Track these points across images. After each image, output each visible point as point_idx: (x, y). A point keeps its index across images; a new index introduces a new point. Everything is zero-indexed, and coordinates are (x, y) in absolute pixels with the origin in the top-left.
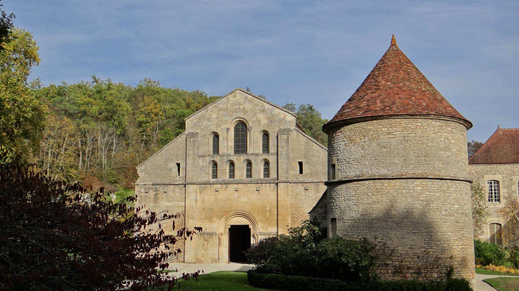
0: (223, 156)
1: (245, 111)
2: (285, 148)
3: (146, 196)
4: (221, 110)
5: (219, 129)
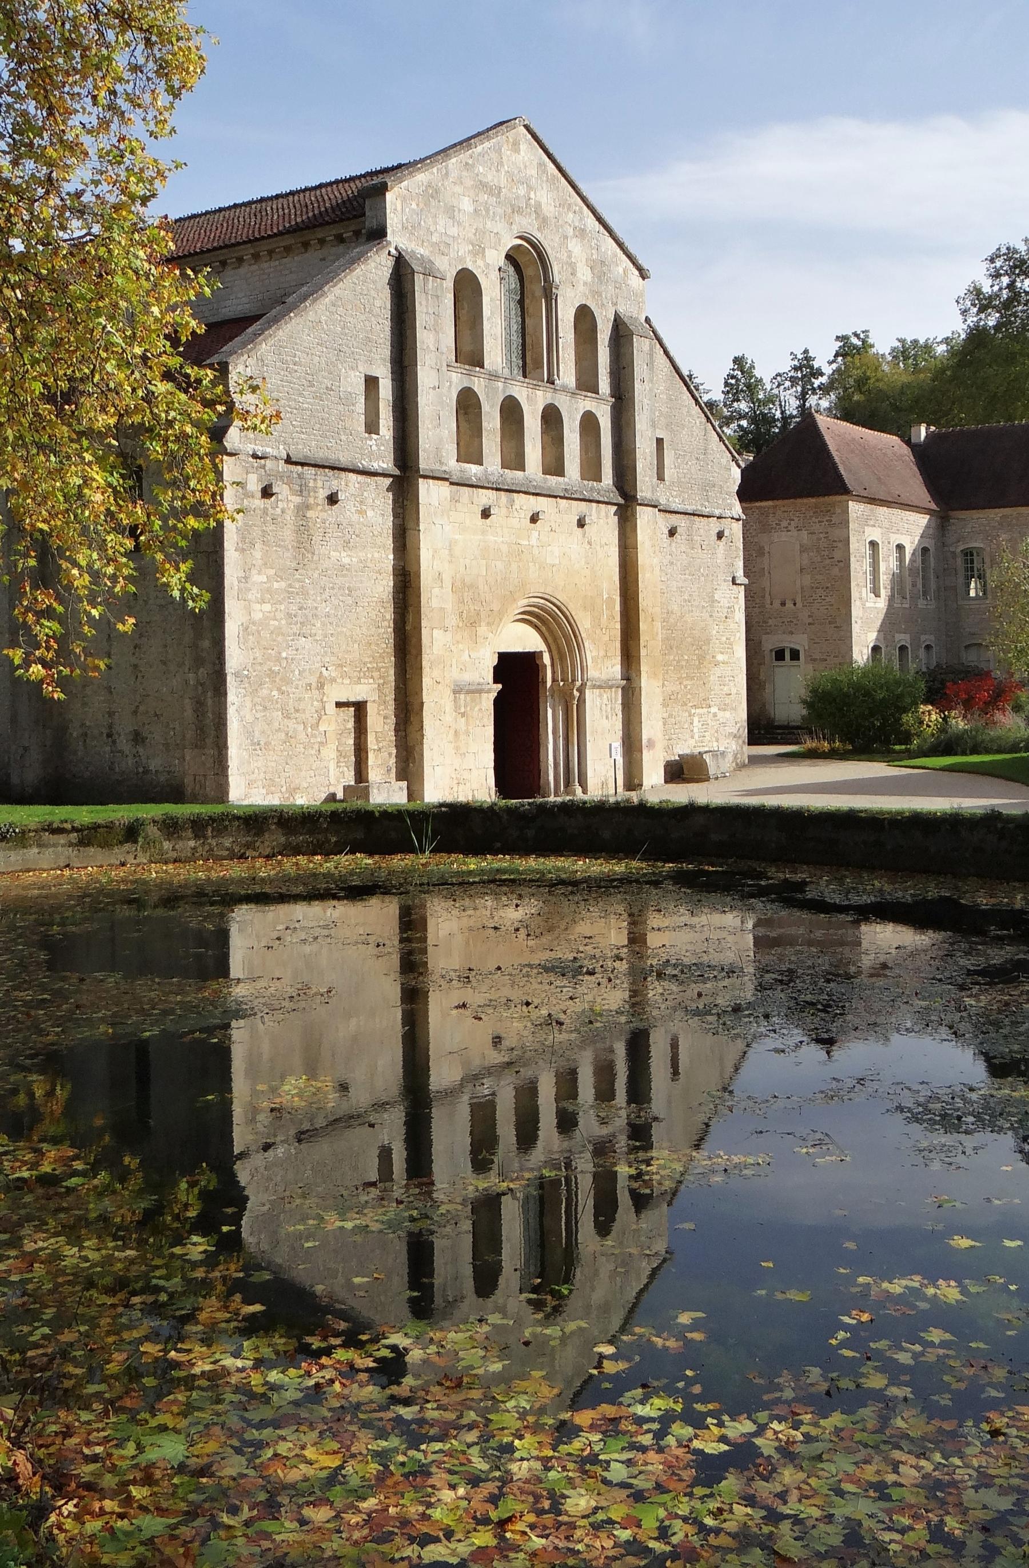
0: (493, 376)
3: (265, 511)
4: (483, 186)
5: (480, 263)
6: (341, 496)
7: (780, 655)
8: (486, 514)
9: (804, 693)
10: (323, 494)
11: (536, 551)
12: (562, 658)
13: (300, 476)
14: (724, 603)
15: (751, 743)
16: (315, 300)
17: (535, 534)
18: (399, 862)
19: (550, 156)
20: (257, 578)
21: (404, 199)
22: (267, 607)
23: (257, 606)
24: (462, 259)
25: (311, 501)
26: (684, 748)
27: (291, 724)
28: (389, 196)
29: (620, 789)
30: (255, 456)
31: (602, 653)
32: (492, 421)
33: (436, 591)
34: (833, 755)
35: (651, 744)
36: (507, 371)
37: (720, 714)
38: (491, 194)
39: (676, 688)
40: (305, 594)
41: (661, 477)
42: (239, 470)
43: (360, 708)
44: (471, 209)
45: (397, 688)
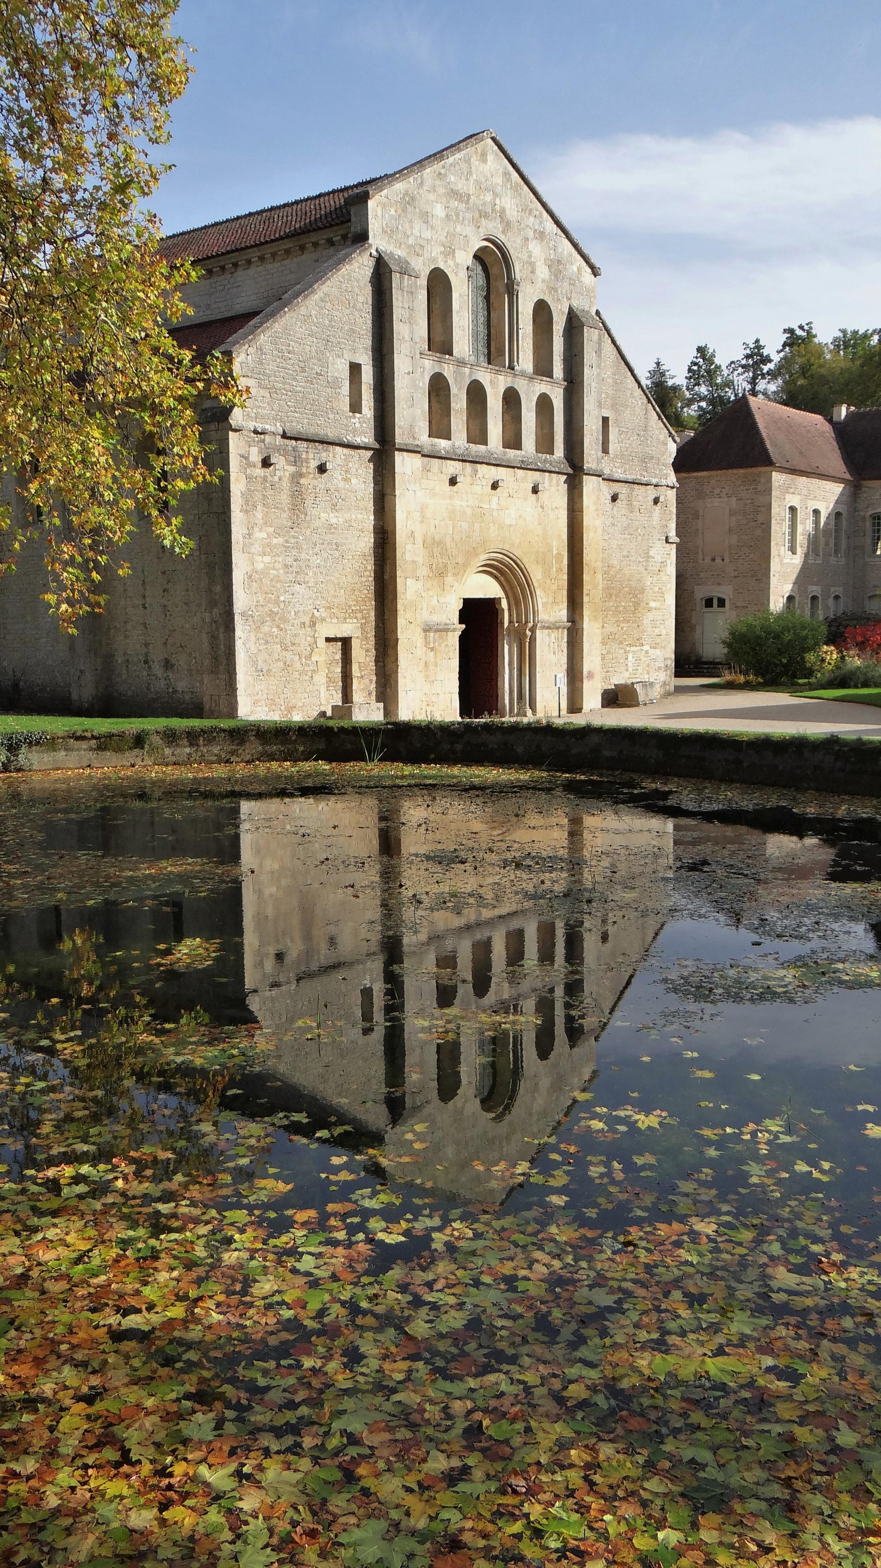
0: (461, 363)
1: (507, 225)
2: (595, 371)
3: (265, 479)
4: (453, 194)
6: (329, 466)
7: (709, 603)
8: (453, 482)
9: (725, 635)
10: (314, 464)
11: (495, 513)
12: (517, 603)
13: (294, 449)
14: (658, 558)
15: (678, 674)
16: (306, 297)
17: (495, 499)
18: (351, 768)
19: (514, 166)
20: (260, 535)
21: (384, 206)
22: (267, 559)
23: (259, 558)
24: (434, 260)
25: (304, 470)
26: (619, 679)
27: (289, 656)
28: (371, 203)
29: (564, 712)
30: (256, 432)
31: (551, 600)
32: (459, 402)
33: (409, 547)
34: (747, 686)
35: (591, 675)
36: (472, 358)
37: (651, 651)
38: (461, 200)
39: (614, 629)
40: (299, 548)
41: (605, 450)
42: (242, 443)
43: (346, 643)
44: (443, 215)
45: (377, 627)
